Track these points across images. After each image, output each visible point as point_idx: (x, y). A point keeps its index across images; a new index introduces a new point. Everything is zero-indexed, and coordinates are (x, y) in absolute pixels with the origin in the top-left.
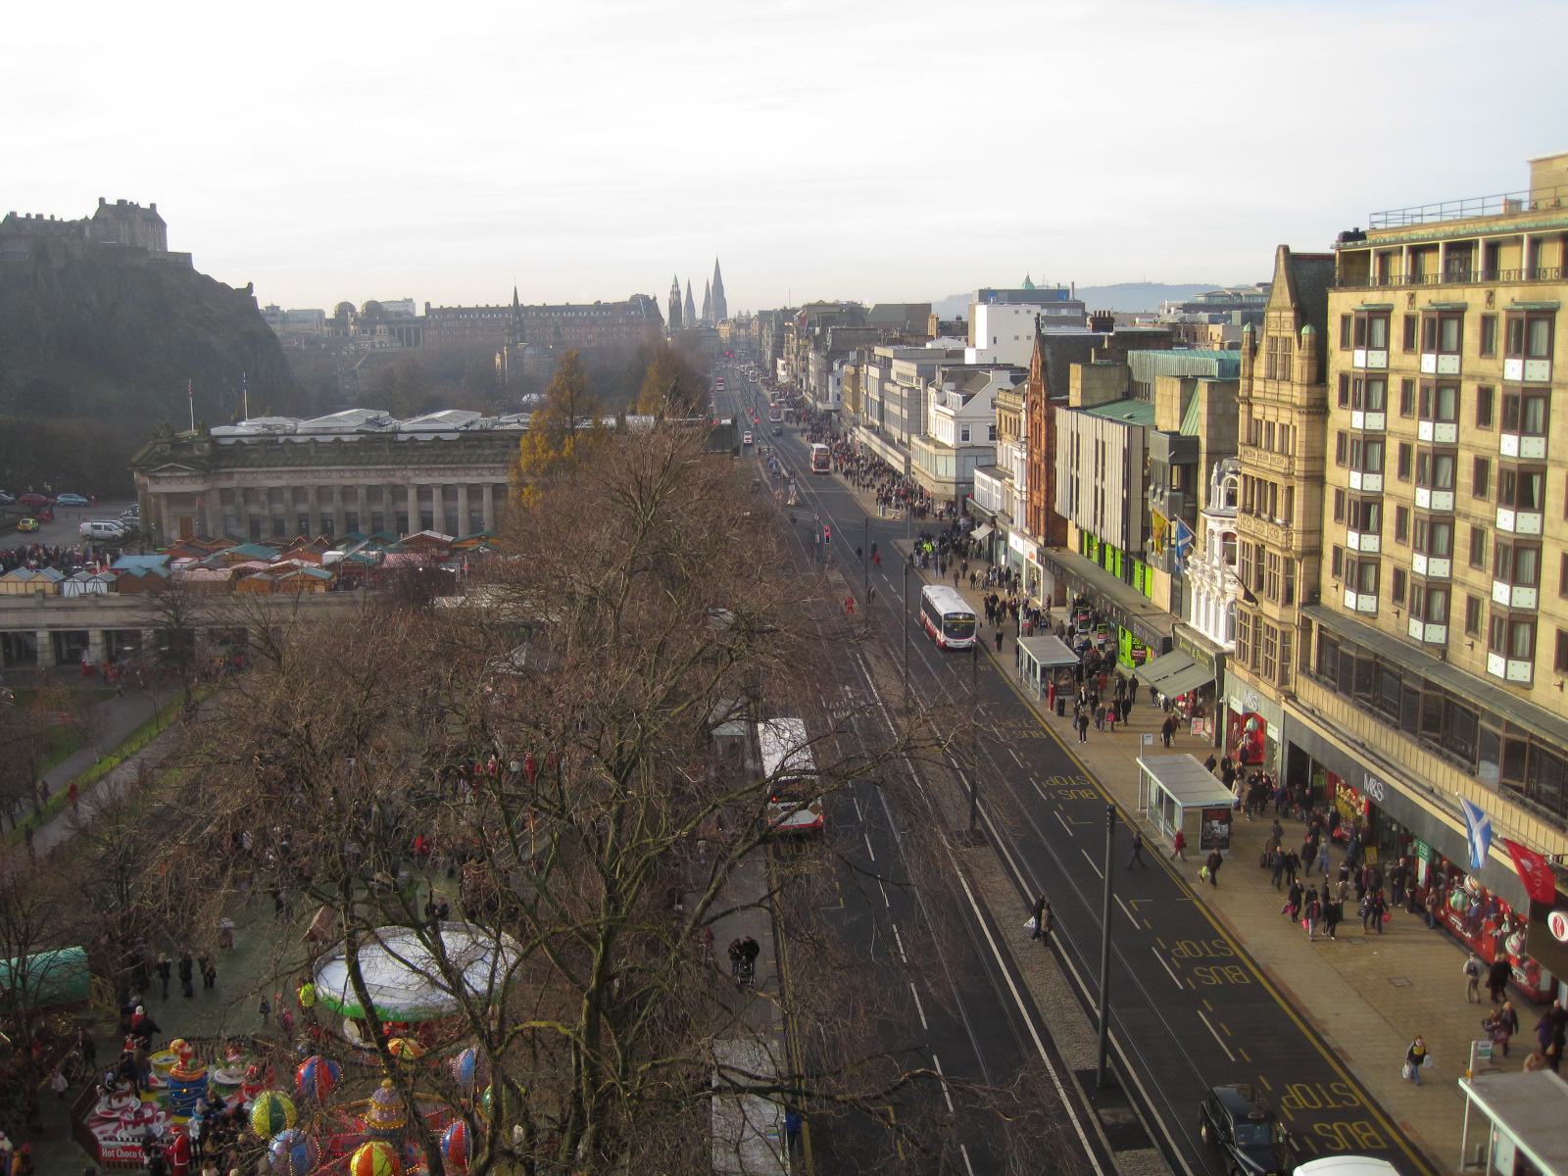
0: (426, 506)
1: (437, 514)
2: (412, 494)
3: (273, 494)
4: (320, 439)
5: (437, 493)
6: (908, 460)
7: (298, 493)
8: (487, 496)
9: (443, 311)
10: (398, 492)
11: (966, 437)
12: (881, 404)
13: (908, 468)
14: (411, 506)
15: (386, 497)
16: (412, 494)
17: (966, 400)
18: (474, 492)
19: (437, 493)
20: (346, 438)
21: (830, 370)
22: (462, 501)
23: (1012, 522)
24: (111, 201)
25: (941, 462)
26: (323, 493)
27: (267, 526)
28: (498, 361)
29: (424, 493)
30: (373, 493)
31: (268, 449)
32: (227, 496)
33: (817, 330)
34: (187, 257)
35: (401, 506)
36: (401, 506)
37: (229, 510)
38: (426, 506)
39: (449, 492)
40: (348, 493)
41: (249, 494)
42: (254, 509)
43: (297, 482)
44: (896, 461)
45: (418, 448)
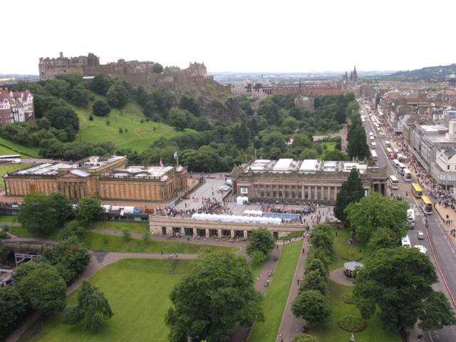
2: (303, 188)
3: (267, 186)
4: (280, 172)
5: (309, 188)
7: (274, 186)
10: (300, 187)
12: (420, 146)
14: (303, 191)
17: (449, 158)
18: (319, 188)
19: (309, 188)
21: (398, 119)
22: (316, 190)
24: (193, 63)
26: (280, 186)
27: (265, 194)
29: (306, 187)
30: (293, 187)
31: (267, 174)
32: (255, 186)
33: (393, 104)
34: (212, 76)
35: (300, 190)
37: (256, 189)
38: (306, 190)
39: (312, 187)
40: (286, 186)
41: (261, 186)
42: (262, 189)
43: (274, 184)
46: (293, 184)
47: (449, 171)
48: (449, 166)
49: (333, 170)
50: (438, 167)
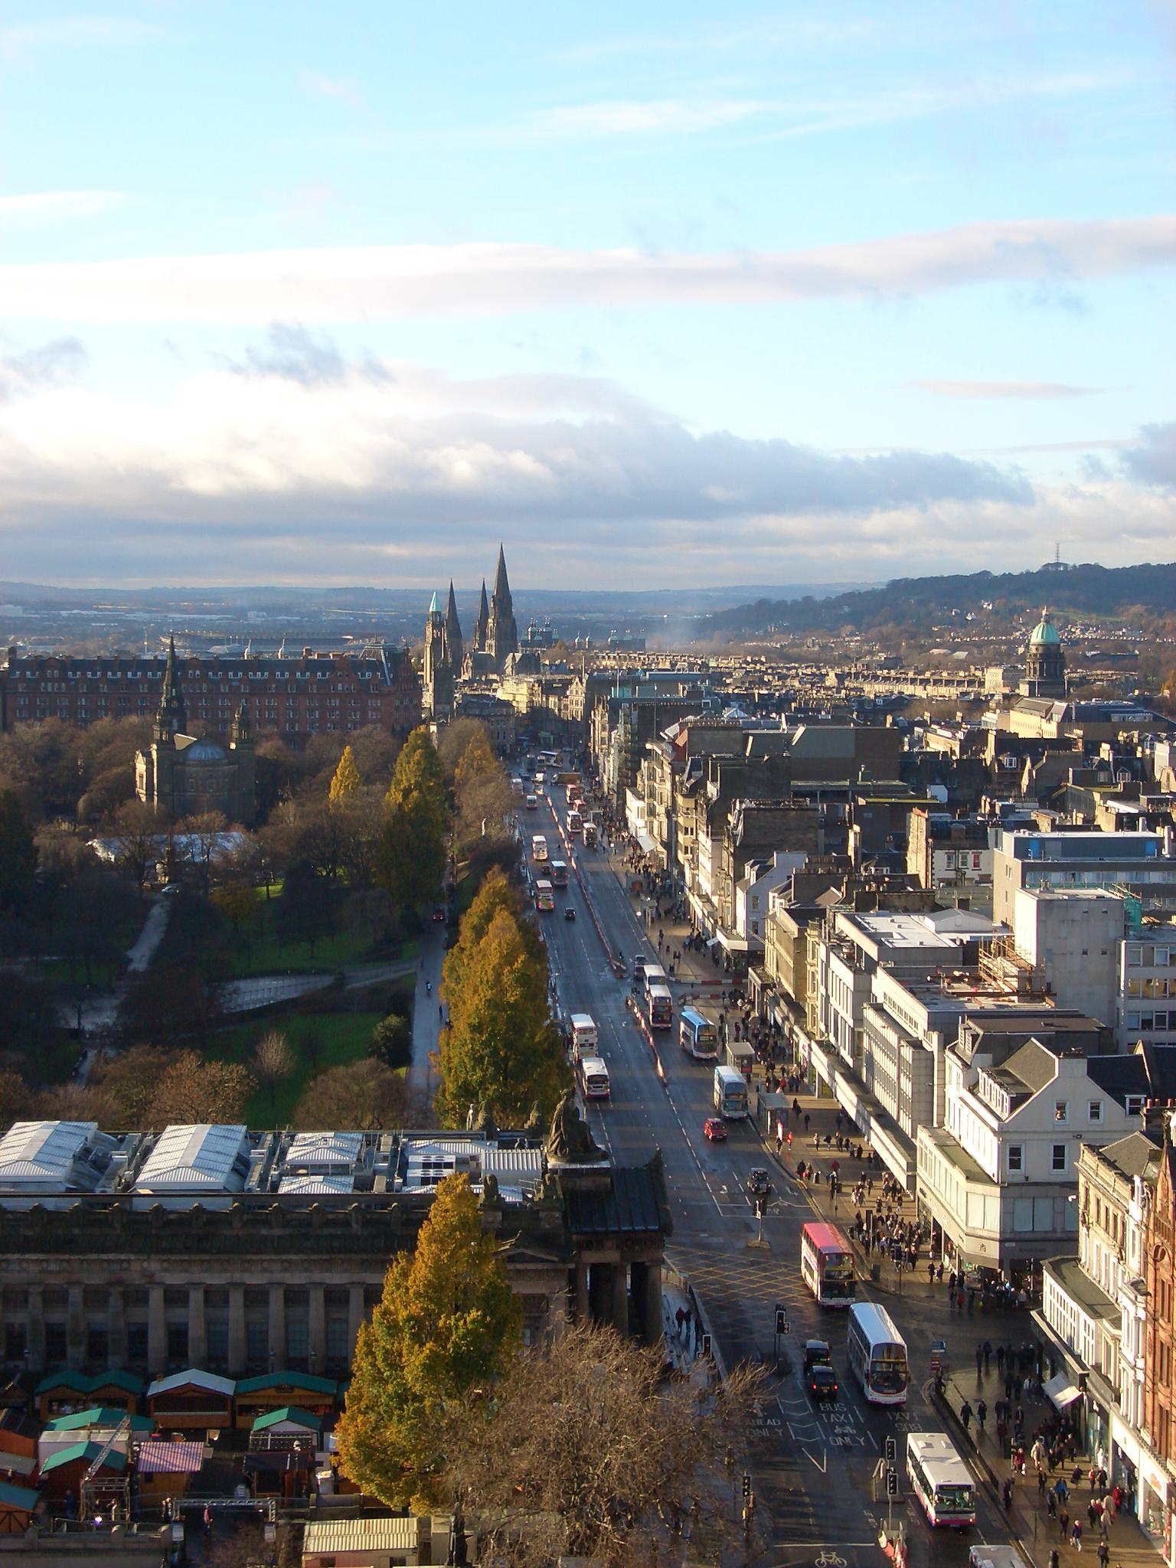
0: (177, 1314)
1: (196, 1330)
2: (156, 1297)
6: (912, 1167)
8: (276, 1303)
9: (40, 664)
11: (1015, 1164)
13: (912, 1180)
14: (155, 1314)
15: (115, 1301)
16: (156, 1297)
19: (196, 1297)
20: (50, 1204)
22: (236, 1310)
23: (1118, 1399)
25: (976, 1204)
28: (141, 767)
30: (95, 1297)
35: (137, 1315)
36: (137, 1315)
38: (177, 1314)
44: (895, 1161)
45: (169, 1223)
46: (96, 1279)
47: (1017, 1175)
48: (1015, 1152)
49: (341, 1187)
50: (952, 1150)
